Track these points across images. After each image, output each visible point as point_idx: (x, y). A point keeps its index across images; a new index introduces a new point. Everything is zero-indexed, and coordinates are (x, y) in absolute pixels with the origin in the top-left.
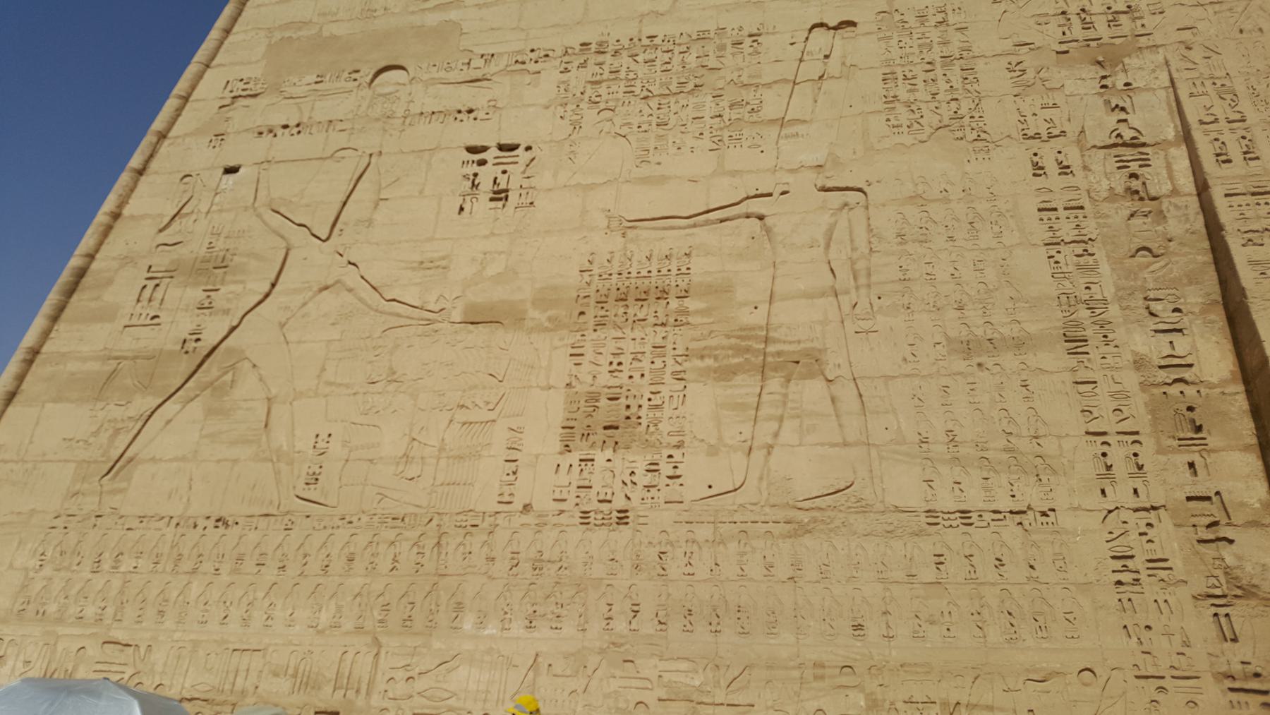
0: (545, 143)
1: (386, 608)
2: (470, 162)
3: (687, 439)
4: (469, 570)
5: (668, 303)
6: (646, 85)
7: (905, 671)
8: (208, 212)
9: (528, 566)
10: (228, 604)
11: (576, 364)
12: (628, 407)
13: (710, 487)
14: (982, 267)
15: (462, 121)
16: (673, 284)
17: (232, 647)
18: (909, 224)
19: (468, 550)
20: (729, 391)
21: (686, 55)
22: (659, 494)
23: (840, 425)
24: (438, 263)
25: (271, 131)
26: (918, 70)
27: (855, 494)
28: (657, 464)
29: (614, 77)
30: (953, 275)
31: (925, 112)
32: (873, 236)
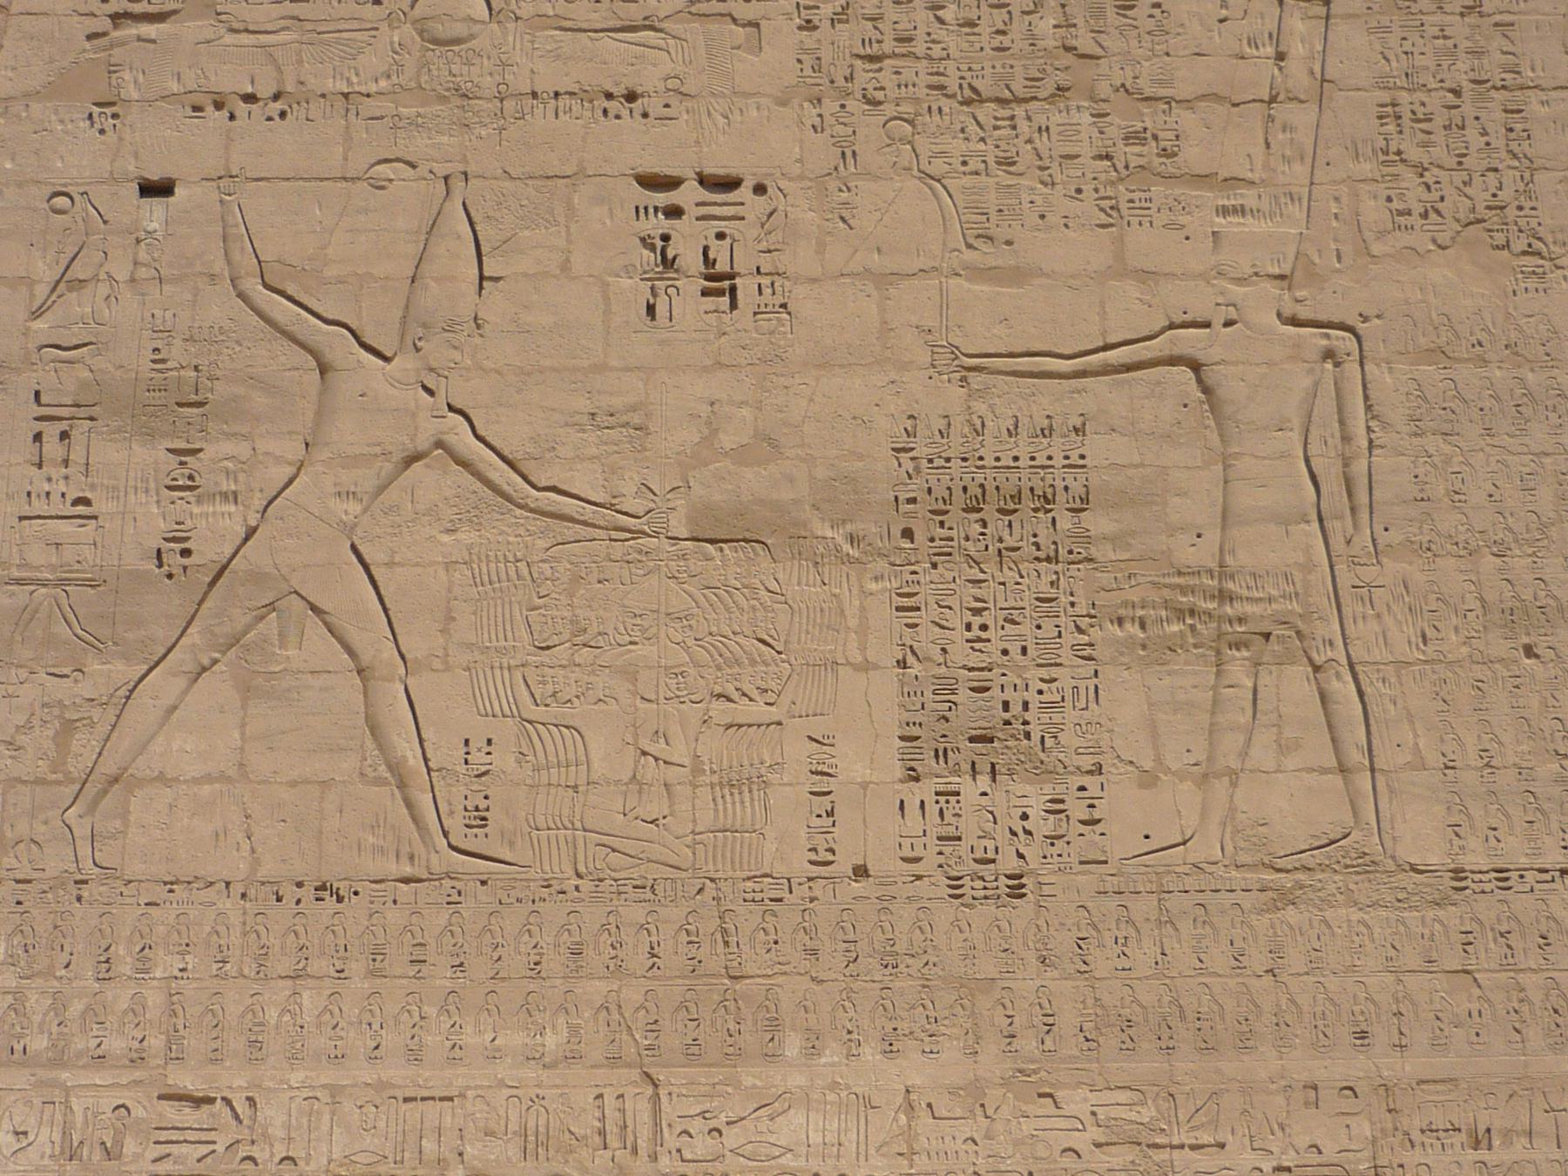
0: (790, 179)
1: (653, 1027)
2: (651, 210)
3: (1107, 760)
4: (777, 968)
5: (1054, 519)
6: (968, 75)
7: (1423, 1091)
8: (133, 280)
9: (874, 963)
10: (376, 1026)
11: (907, 625)
12: (1006, 706)
13: (1147, 837)
14: (1532, 484)
15: (618, 117)
16: (1060, 484)
17: (400, 1094)
18: (1425, 399)
19: (772, 937)
20: (1167, 681)
21: (1034, 18)
22: (1071, 849)
23: (1334, 740)
24: (625, 418)
25: (219, 106)
26: (1435, 101)
27: (1356, 846)
28: (1062, 801)
29: (903, 51)
30: (1491, 496)
31: (1448, 191)
32: (1372, 418)
